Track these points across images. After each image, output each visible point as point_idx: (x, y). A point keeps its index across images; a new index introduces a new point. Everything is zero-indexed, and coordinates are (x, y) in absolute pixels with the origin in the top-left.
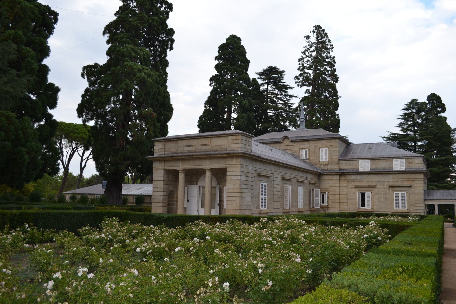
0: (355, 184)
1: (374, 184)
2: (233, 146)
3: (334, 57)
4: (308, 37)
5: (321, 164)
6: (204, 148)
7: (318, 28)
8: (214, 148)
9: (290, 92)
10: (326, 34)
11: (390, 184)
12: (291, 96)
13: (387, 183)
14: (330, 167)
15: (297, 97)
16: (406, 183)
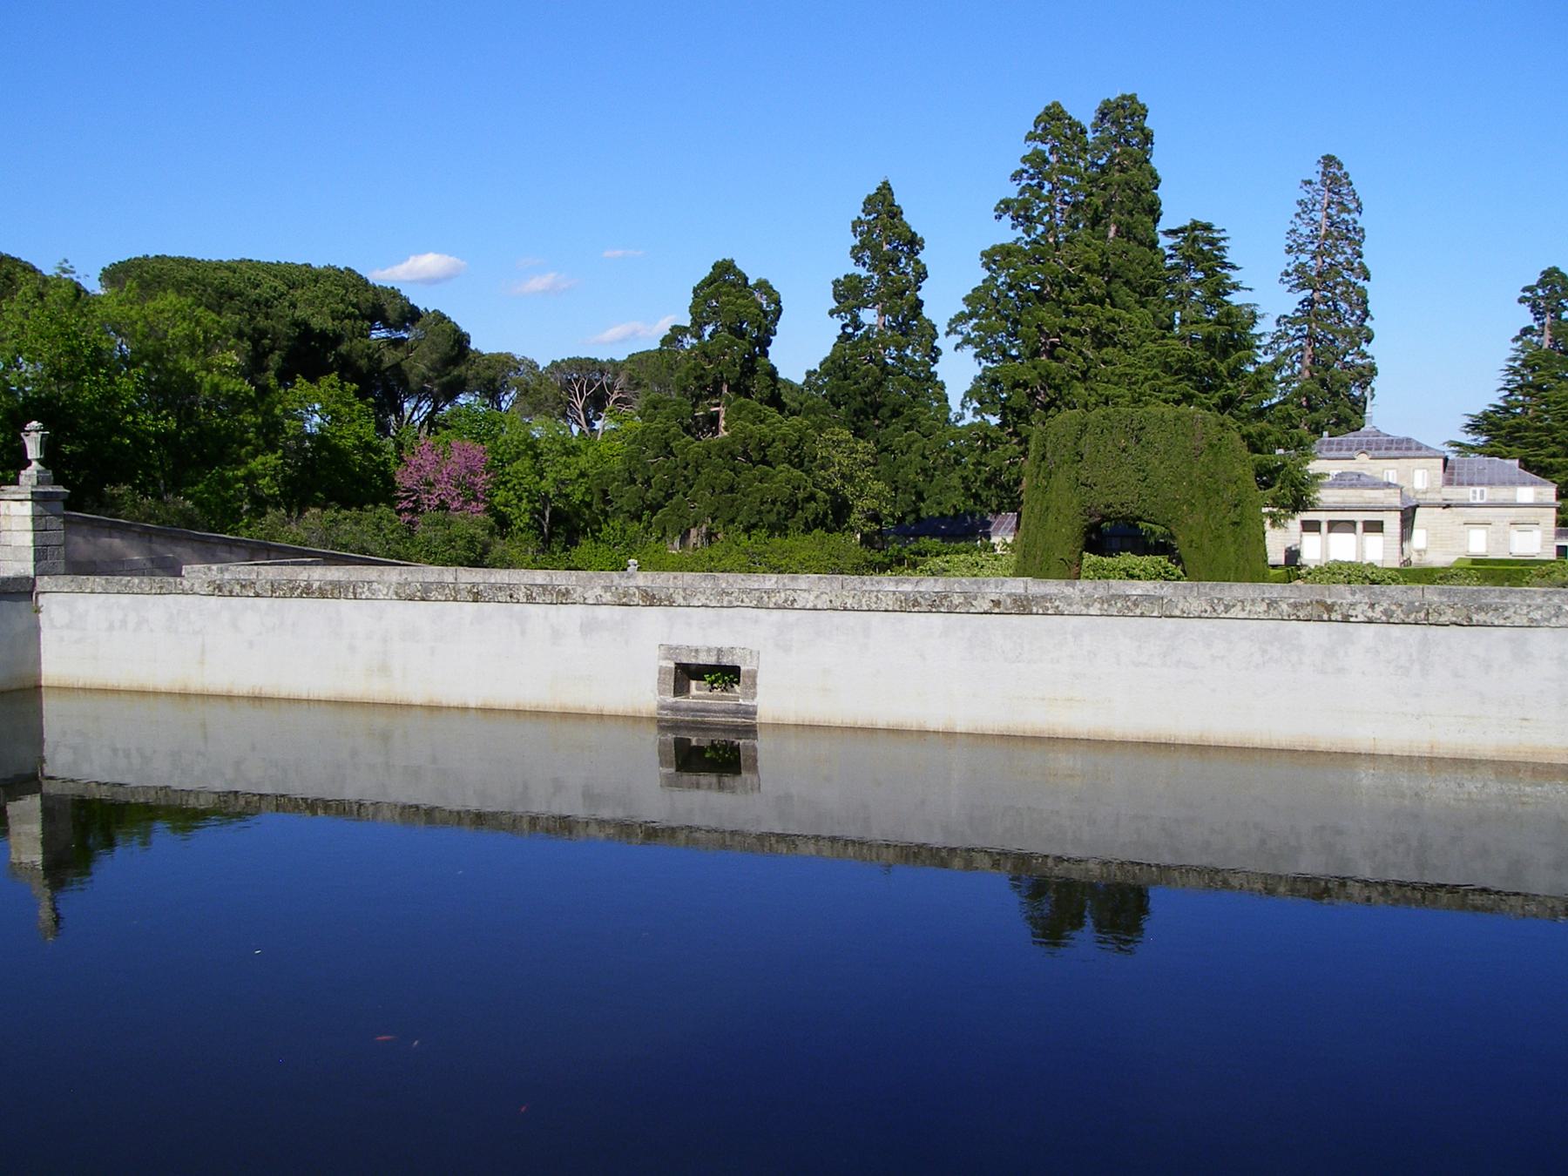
0: (1465, 520)
1: (1491, 520)
2: (1391, 499)
3: (1362, 230)
4: (1309, 183)
5: (1417, 492)
6: (1354, 499)
7: (1329, 160)
8: (1368, 500)
9: (1235, 277)
10: (1346, 175)
11: (1513, 519)
12: (1236, 287)
13: (1508, 519)
14: (1428, 496)
15: (1251, 289)
16: (1532, 519)
